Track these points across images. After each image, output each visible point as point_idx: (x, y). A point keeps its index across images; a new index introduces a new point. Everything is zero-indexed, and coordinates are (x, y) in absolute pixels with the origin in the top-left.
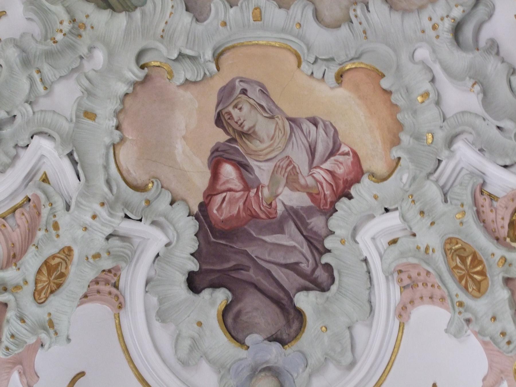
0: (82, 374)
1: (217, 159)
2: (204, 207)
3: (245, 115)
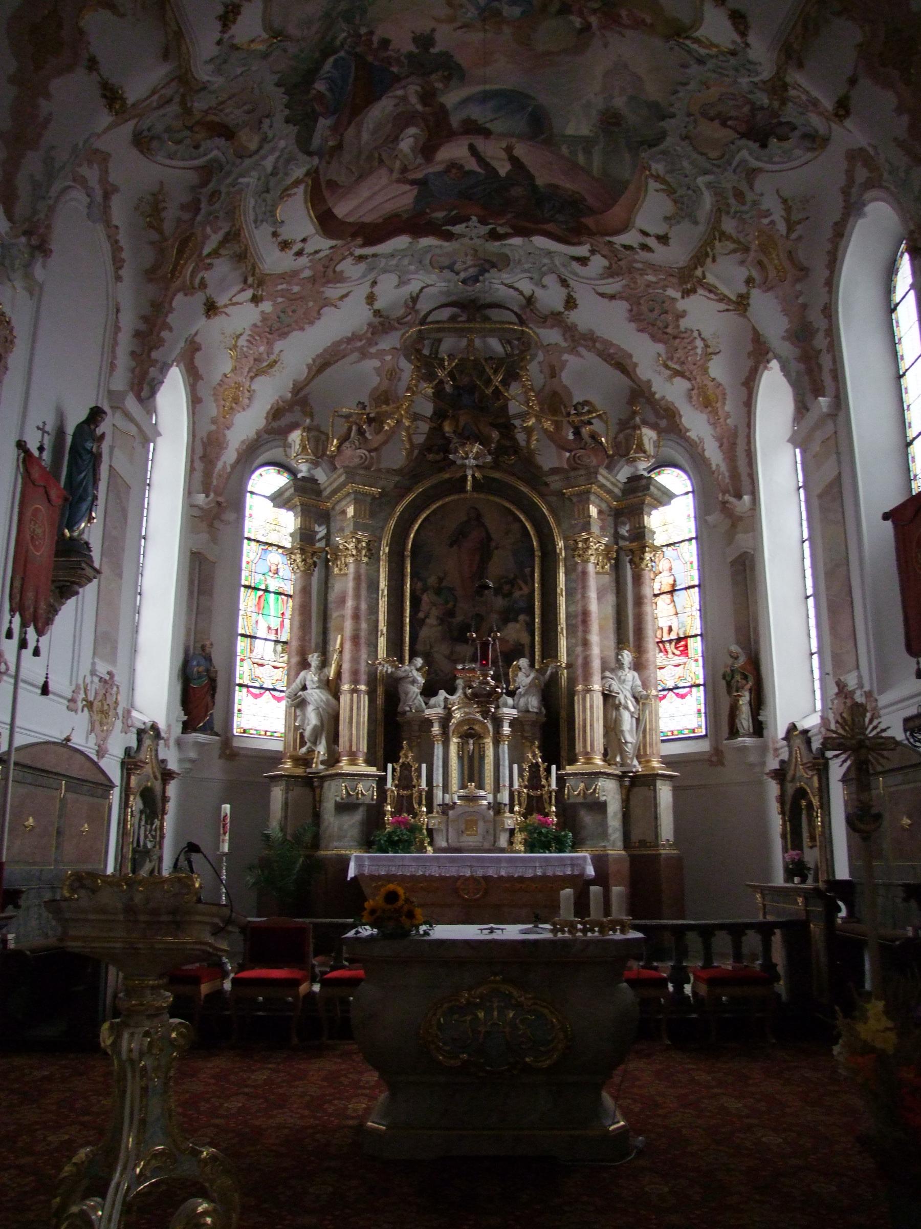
0: (778, 191)
1: (724, 124)
2: (739, 133)
3: (712, 113)
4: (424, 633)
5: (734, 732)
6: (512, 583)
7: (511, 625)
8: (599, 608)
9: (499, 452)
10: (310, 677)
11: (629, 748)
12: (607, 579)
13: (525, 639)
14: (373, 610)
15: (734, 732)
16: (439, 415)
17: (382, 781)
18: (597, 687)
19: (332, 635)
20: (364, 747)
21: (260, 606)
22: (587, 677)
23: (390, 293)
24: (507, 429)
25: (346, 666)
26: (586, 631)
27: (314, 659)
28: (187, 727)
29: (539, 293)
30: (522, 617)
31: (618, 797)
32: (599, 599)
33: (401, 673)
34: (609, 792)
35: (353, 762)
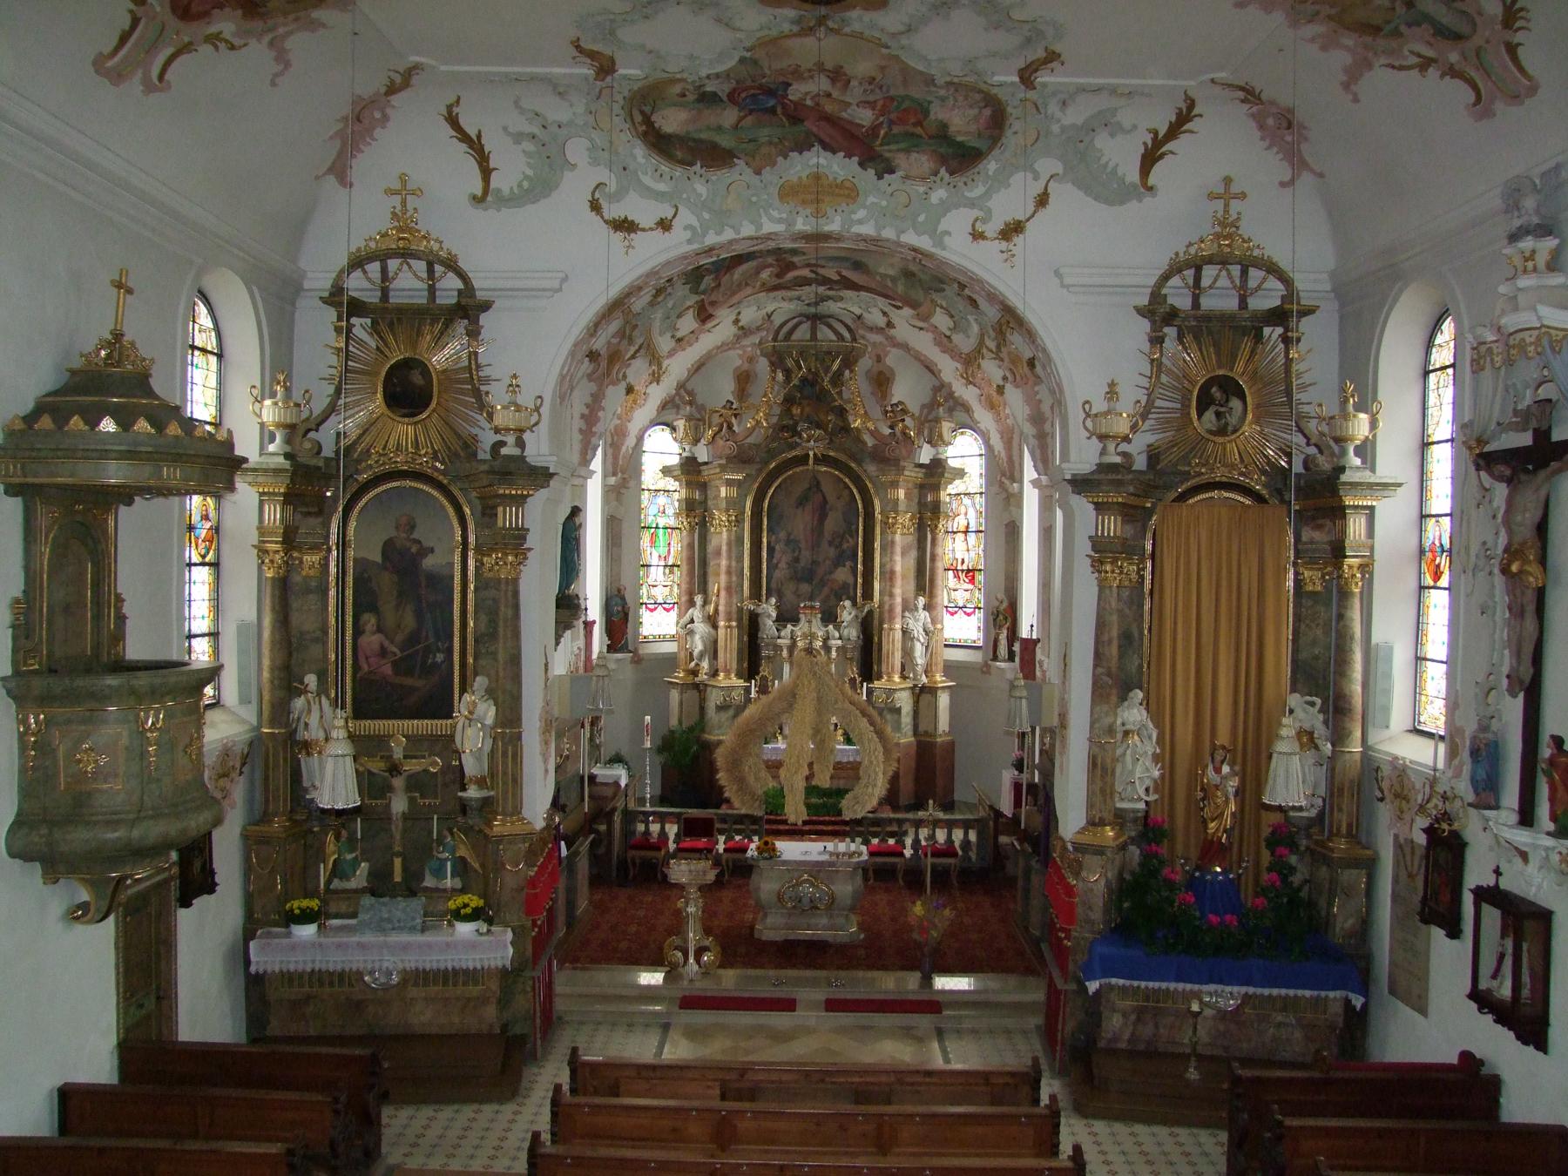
4: (777, 574)
5: (995, 658)
6: (843, 537)
7: (840, 569)
8: (902, 564)
9: (832, 436)
10: (696, 613)
11: (919, 669)
12: (911, 539)
13: (850, 580)
14: (740, 559)
15: (995, 658)
16: (789, 401)
17: (748, 690)
18: (898, 626)
19: (711, 579)
20: (735, 666)
21: (653, 542)
22: (892, 619)
23: (750, 315)
24: (842, 412)
25: (721, 608)
26: (892, 586)
27: (699, 599)
28: (611, 649)
29: (866, 315)
30: (848, 564)
31: (911, 701)
32: (903, 554)
33: (759, 610)
34: (904, 701)
35: (728, 676)
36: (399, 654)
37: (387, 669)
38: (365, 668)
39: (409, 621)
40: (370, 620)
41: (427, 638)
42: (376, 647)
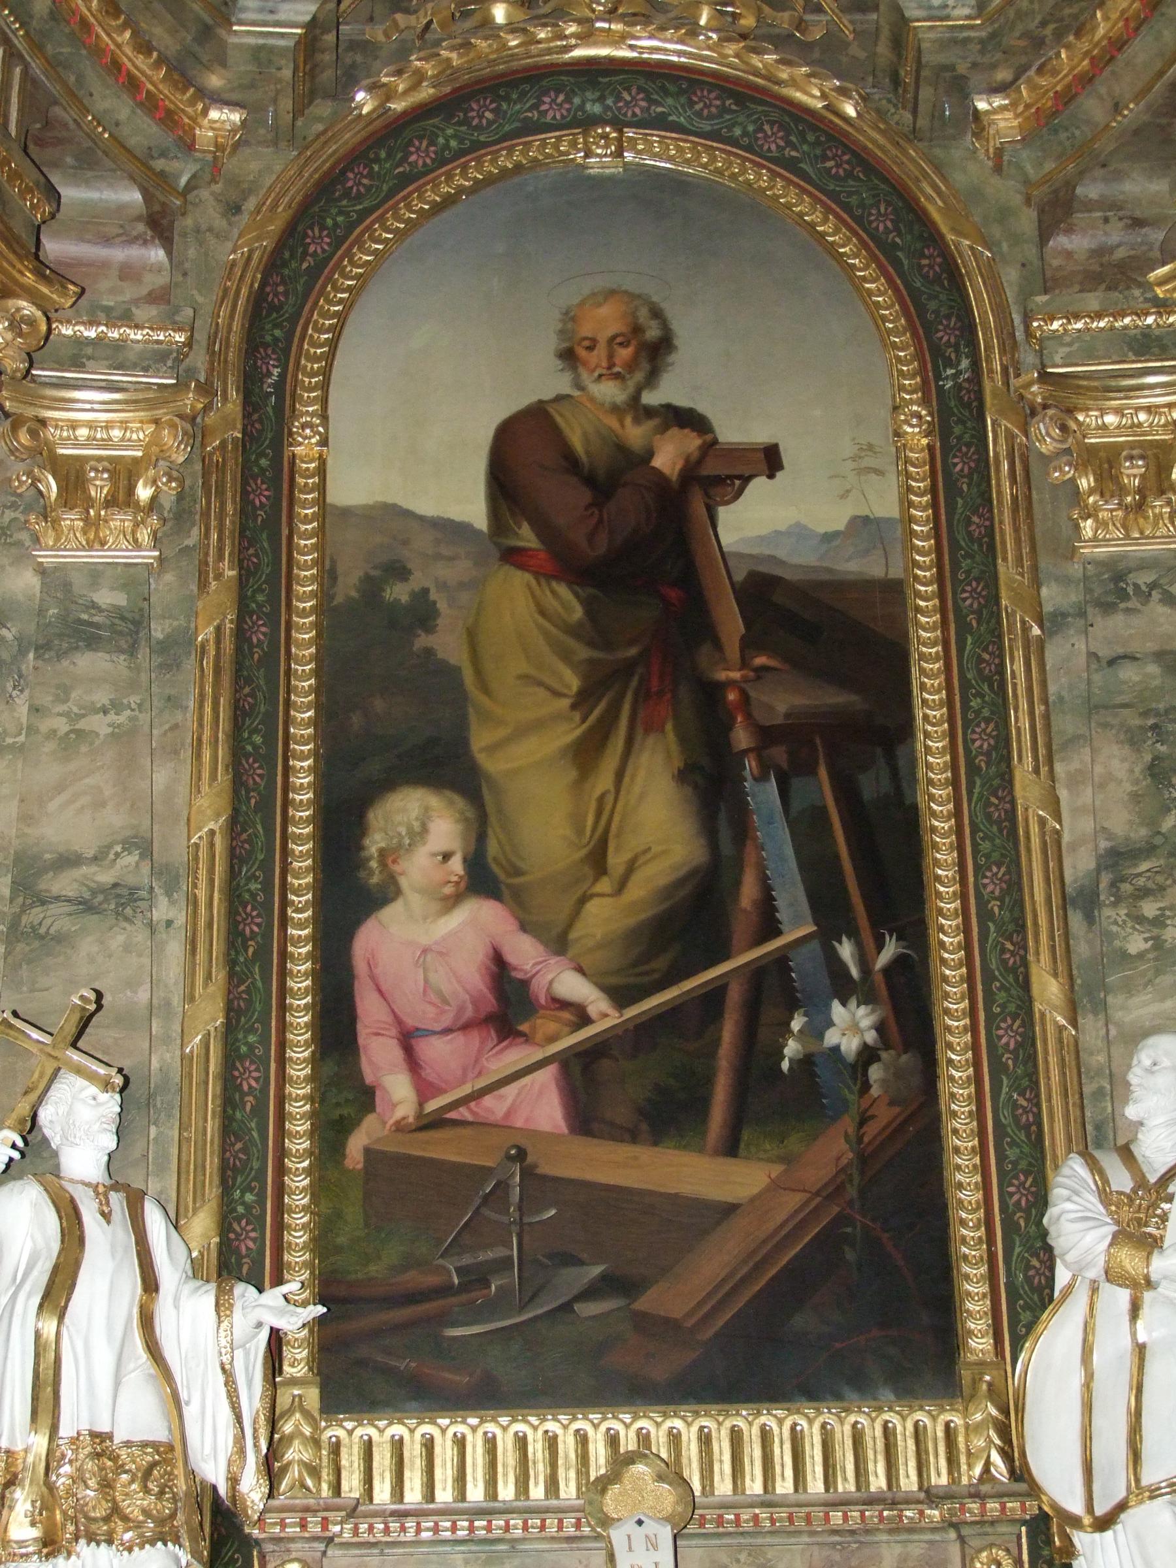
36: (605, 1015)
37: (539, 1105)
38: (398, 1093)
39: (659, 828)
40: (420, 831)
41: (769, 927)
42: (464, 977)
